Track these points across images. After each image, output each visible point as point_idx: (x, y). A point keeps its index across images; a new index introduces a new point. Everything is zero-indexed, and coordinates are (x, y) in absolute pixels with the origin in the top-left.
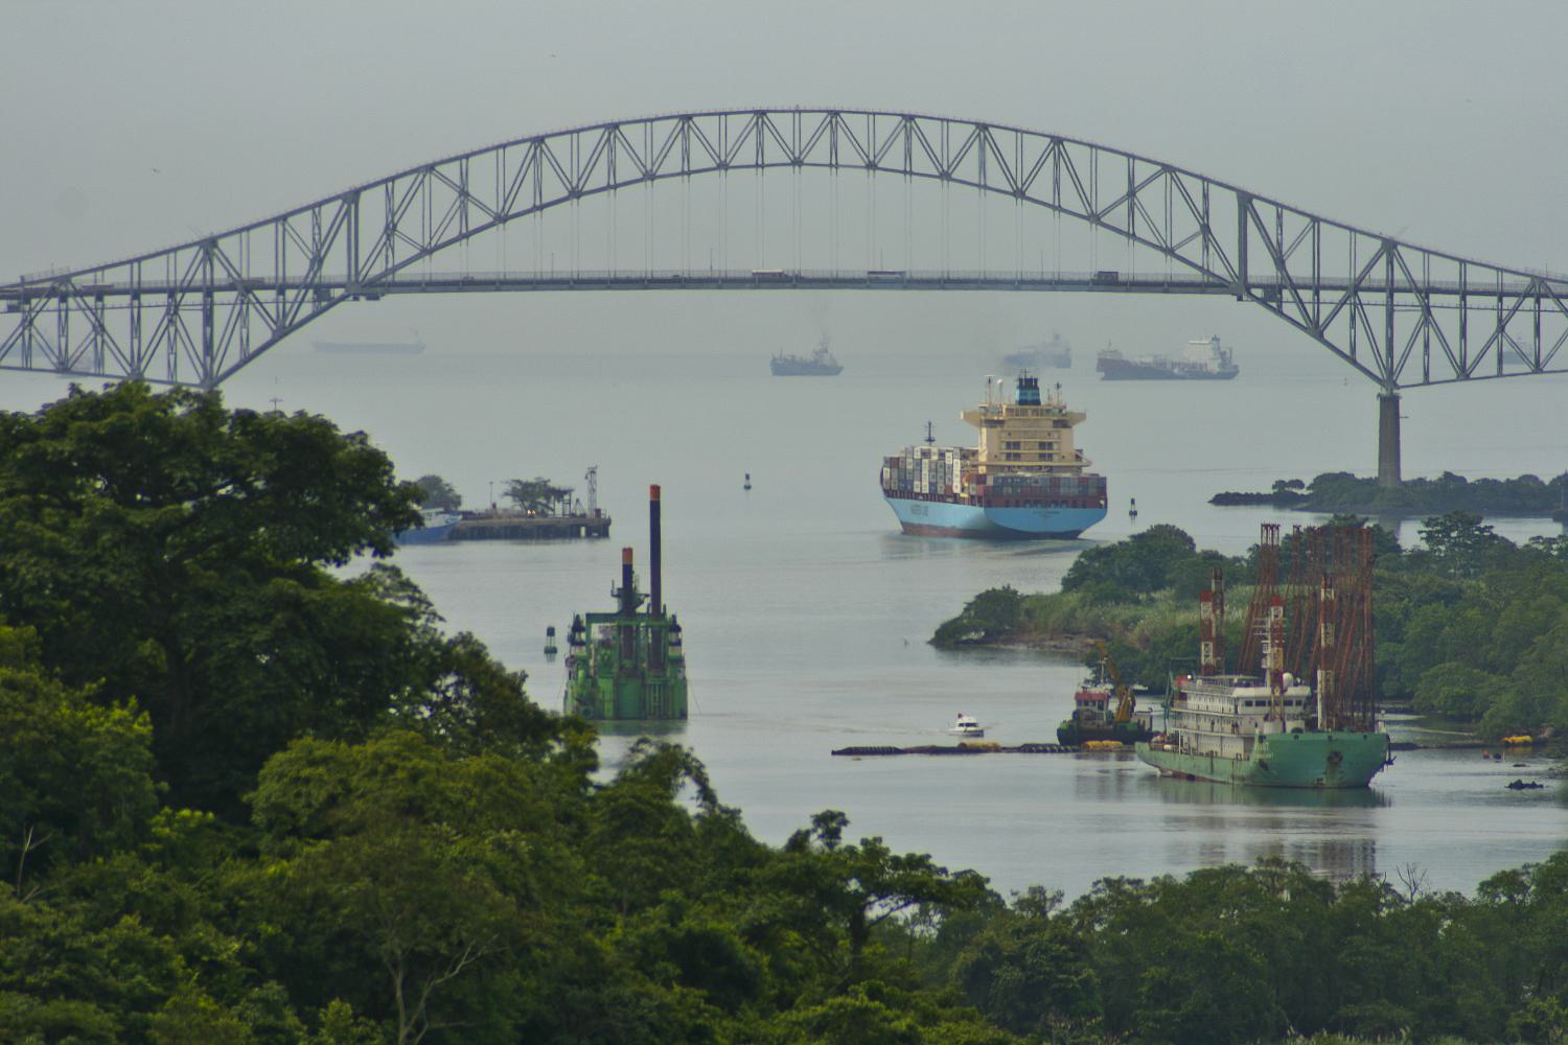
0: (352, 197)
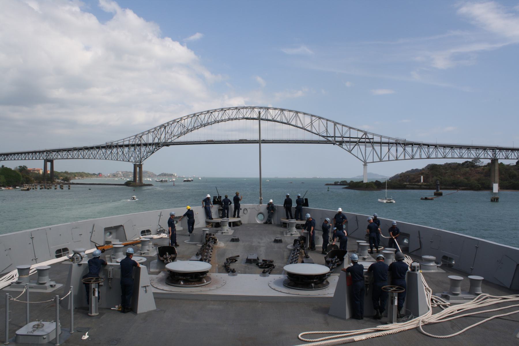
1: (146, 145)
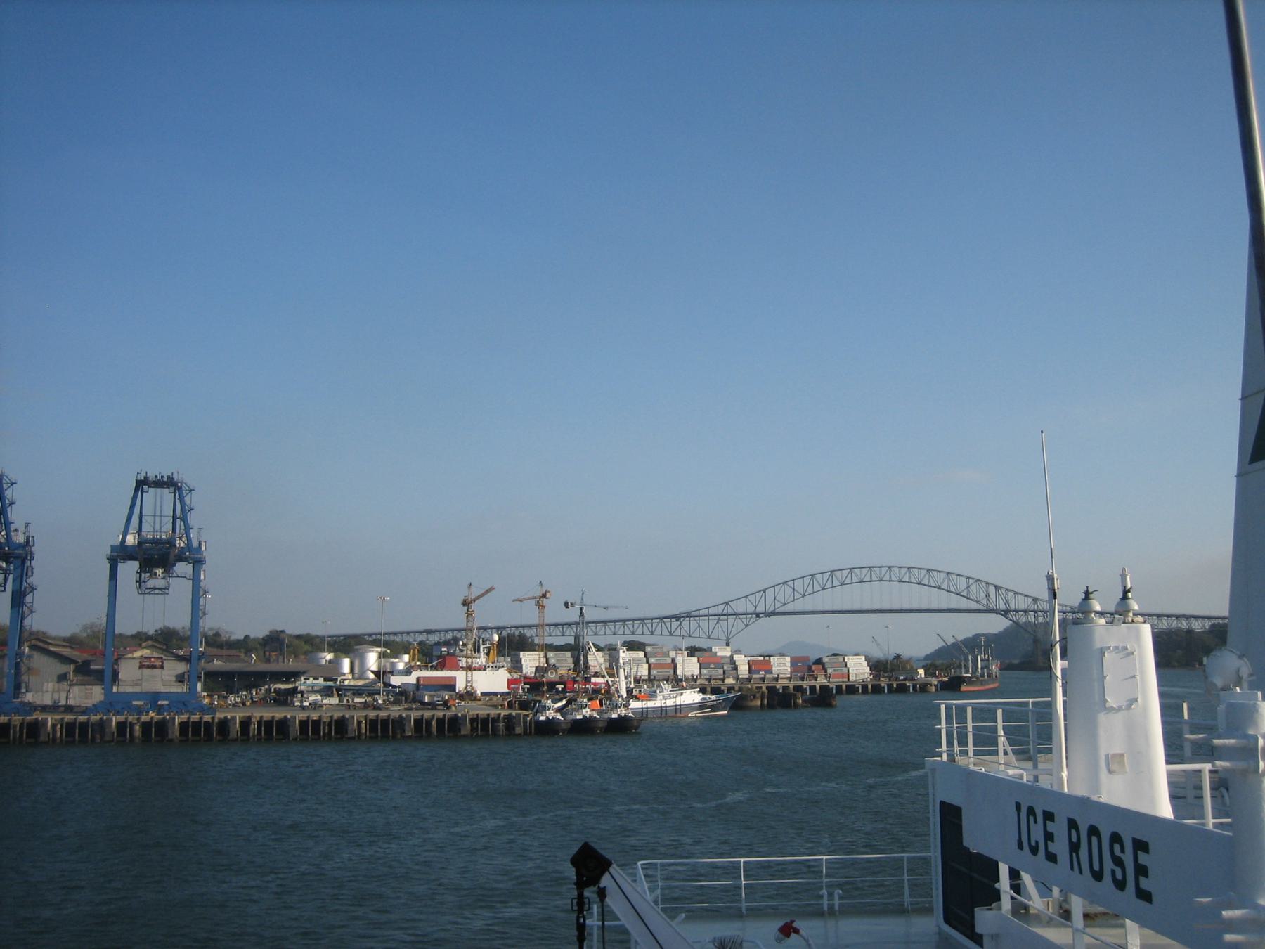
0: (764, 591)
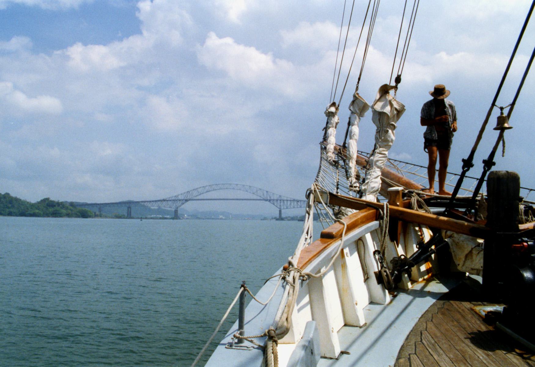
0: (189, 192)
1: (180, 200)
